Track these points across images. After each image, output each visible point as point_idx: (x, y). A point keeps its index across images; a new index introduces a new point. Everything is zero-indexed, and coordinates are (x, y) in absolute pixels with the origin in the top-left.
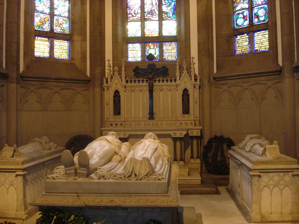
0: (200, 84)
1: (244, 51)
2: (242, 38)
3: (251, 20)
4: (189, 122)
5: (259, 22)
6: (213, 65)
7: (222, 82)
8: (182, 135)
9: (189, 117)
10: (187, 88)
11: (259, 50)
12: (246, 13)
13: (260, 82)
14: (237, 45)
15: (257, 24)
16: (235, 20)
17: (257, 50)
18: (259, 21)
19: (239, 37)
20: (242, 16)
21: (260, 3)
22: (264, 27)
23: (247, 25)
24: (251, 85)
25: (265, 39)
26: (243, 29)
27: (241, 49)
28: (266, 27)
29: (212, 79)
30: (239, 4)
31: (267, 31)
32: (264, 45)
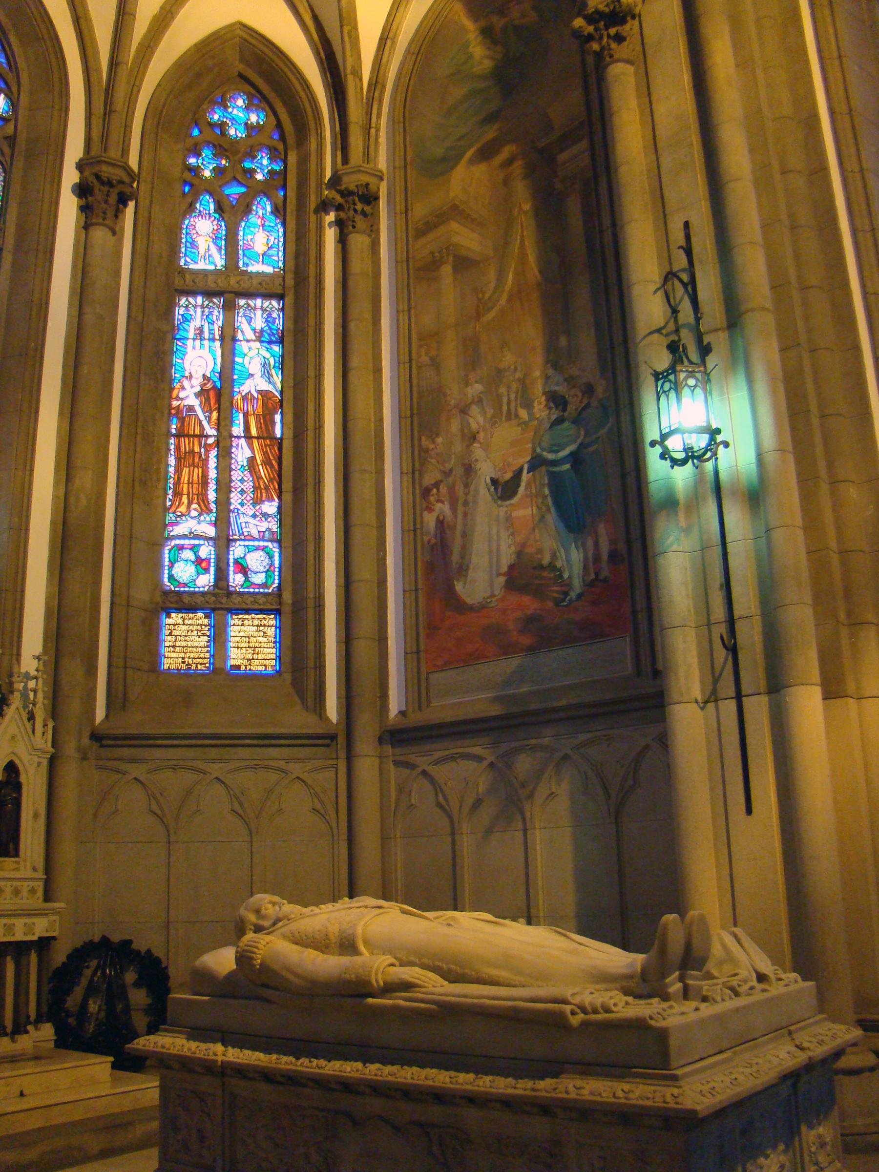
0: (52, 750)
1: (190, 661)
2: (186, 622)
3: (221, 575)
4: (25, 884)
5: (248, 587)
6: (93, 690)
7: (126, 752)
8: (34, 934)
9: (17, 869)
10: (17, 762)
11: (243, 668)
12: (206, 551)
13: (266, 763)
14: (168, 641)
15: (241, 590)
16: (167, 563)
17: (237, 667)
18: (248, 584)
19: (176, 618)
20: (193, 558)
21: (255, 533)
22: (264, 604)
23: (207, 587)
24: (238, 769)
25: (265, 640)
26: (197, 595)
27: (182, 655)
28: (271, 604)
29: (86, 741)
30: (184, 518)
31: (272, 616)
32: (260, 656)
